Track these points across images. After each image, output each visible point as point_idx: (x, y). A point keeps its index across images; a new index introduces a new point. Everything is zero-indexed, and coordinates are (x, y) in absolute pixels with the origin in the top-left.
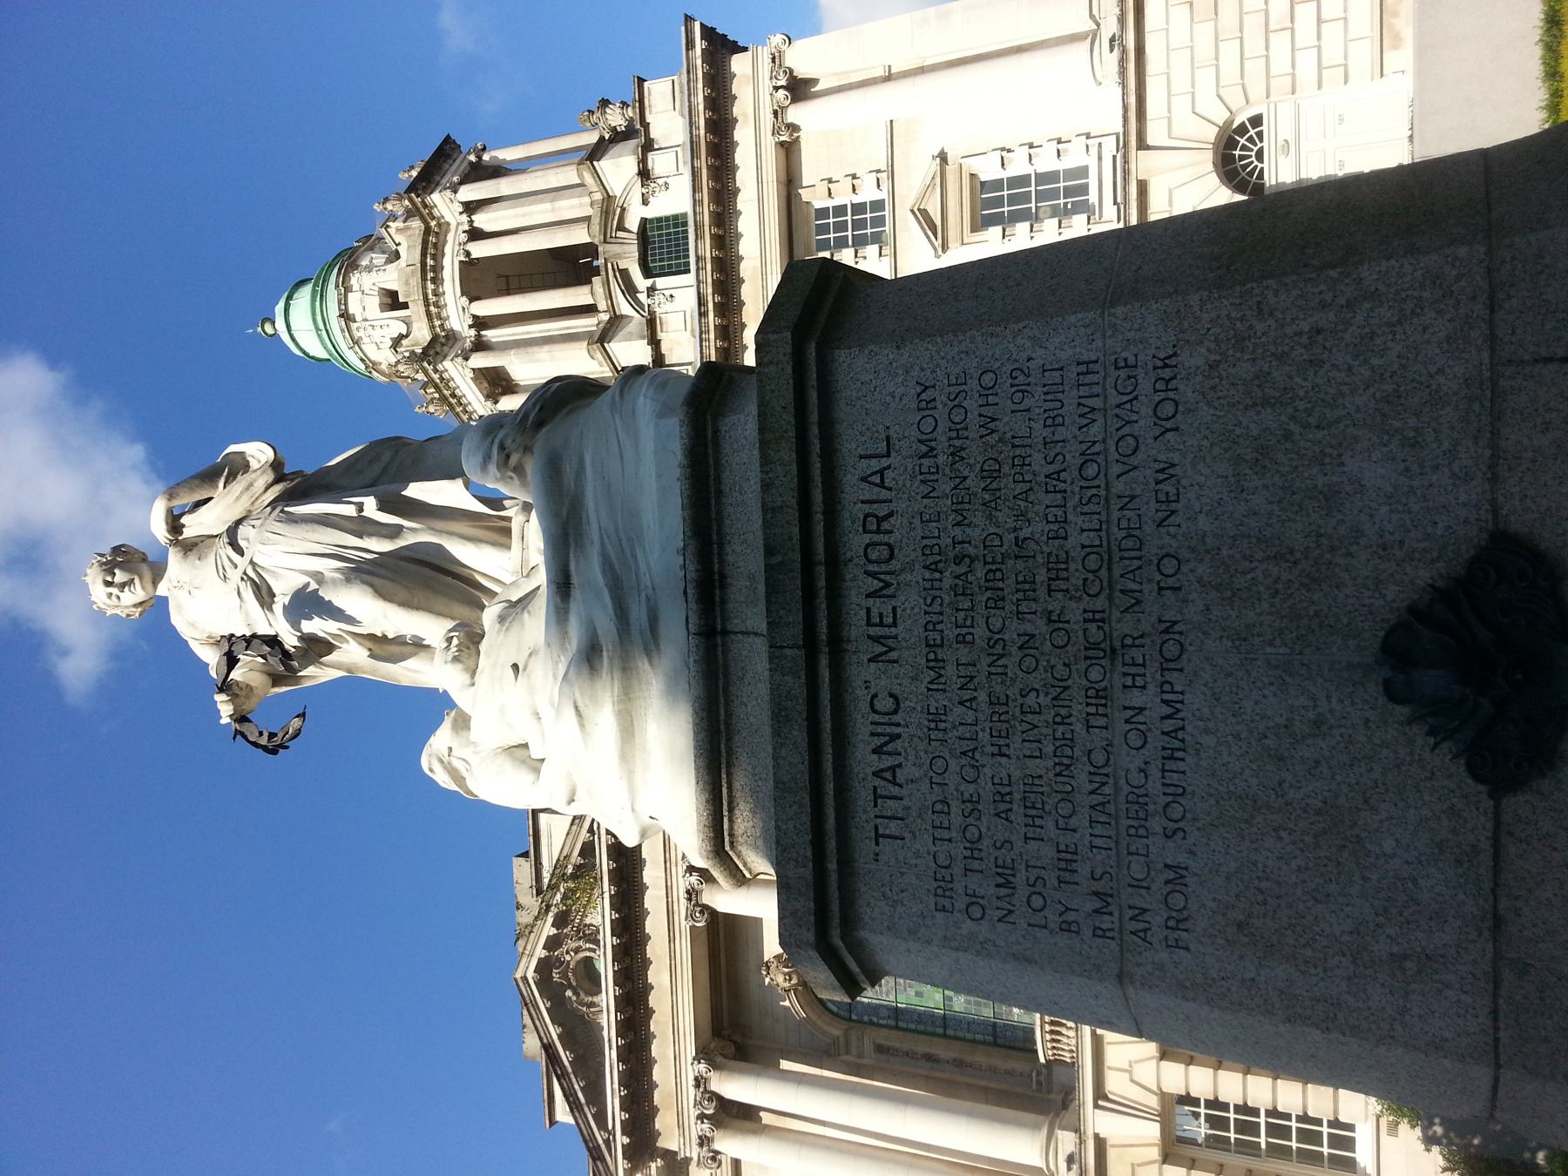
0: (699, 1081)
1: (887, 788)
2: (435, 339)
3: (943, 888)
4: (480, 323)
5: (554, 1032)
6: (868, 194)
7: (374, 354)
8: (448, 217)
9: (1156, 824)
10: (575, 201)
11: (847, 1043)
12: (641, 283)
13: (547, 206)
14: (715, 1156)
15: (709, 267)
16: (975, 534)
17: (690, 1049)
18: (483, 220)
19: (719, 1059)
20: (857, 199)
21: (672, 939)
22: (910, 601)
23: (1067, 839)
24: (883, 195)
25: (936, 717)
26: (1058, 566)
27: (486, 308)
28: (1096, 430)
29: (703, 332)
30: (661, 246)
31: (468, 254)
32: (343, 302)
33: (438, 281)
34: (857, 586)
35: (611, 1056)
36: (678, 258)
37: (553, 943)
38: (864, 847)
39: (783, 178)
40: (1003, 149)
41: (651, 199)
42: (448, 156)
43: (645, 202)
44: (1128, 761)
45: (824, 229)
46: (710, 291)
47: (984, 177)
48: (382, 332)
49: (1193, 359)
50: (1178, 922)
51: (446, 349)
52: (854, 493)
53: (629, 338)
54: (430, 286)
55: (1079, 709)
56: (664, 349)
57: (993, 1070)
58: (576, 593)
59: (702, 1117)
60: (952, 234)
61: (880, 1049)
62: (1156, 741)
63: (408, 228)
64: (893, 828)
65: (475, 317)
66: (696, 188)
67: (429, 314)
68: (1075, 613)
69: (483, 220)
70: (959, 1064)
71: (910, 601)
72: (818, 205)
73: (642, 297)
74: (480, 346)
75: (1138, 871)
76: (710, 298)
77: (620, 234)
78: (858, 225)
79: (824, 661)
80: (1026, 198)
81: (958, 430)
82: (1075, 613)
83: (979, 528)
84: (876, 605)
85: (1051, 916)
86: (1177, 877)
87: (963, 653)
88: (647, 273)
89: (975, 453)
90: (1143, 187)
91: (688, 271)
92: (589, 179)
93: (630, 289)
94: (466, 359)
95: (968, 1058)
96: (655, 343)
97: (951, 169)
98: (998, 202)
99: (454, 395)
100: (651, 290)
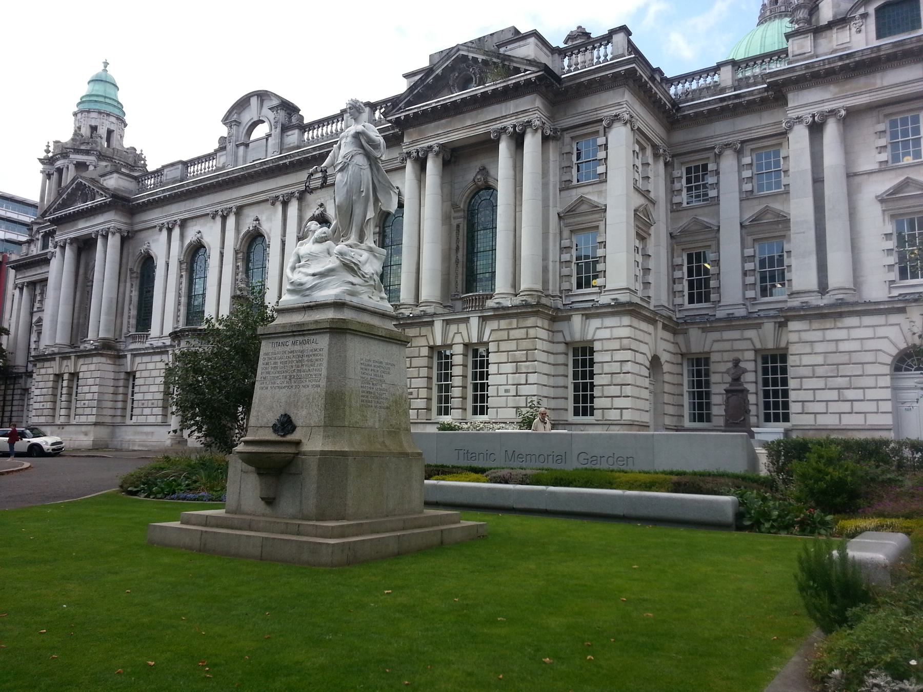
0: (430, 148)
5: (439, 71)
11: (458, 211)
14: (404, 160)
15: (873, 55)
17: (442, 141)
19: (441, 156)
21: (484, 123)
26: (300, 371)
34: (300, 339)
35: (432, 103)
37: (475, 60)
38: (271, 341)
45: (904, 122)
52: (312, 338)
56: (828, 33)
57: (457, 277)
59: (418, 152)
60: (891, 205)
61: (458, 226)
70: (457, 262)
73: (862, 11)
76: (852, 60)
83: (306, 359)
89: (314, 358)
90: (902, 310)
95: (460, 265)
96: (830, 26)
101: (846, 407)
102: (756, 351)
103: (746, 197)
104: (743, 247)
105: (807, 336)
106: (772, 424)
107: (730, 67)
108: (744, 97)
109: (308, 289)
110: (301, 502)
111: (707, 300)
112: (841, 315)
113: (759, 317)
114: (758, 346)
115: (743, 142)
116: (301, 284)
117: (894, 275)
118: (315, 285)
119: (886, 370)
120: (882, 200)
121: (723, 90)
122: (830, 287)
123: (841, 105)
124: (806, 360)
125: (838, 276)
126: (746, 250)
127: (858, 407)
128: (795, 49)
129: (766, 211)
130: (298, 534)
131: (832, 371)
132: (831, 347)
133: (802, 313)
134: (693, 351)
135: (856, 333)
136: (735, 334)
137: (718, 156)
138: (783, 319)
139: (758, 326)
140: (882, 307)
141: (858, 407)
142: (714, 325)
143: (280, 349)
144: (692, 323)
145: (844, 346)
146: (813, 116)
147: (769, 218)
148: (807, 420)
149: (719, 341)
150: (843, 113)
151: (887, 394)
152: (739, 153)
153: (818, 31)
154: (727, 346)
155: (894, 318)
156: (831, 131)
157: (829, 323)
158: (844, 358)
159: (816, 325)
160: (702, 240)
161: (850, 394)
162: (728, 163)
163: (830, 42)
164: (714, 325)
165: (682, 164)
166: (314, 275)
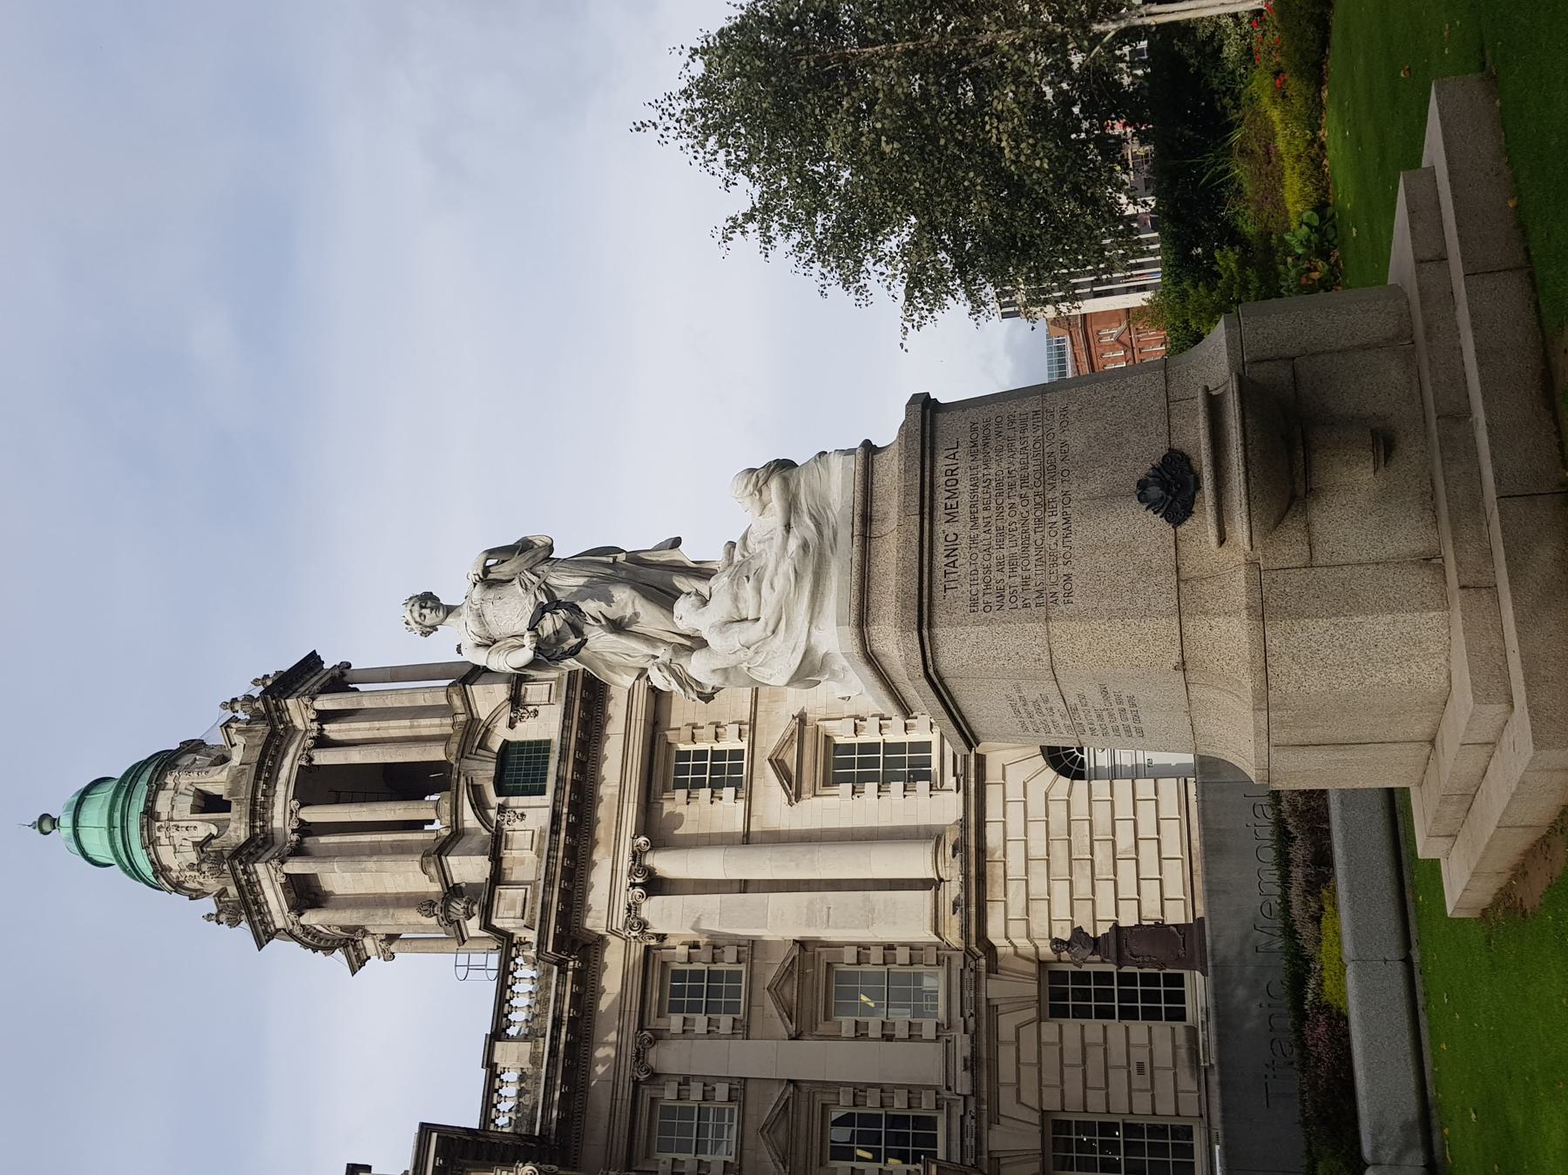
1: (949, 570)
2: (252, 839)
3: (974, 602)
4: (305, 829)
6: (729, 743)
7: (167, 856)
8: (298, 723)
9: (1060, 561)
10: (437, 721)
12: (494, 800)
13: (407, 723)
15: (568, 788)
16: (992, 471)
18: (333, 730)
20: (717, 747)
22: (965, 498)
23: (1026, 574)
24: (744, 745)
25: (973, 540)
26: (1024, 480)
27: (313, 815)
28: (1039, 433)
29: (553, 848)
30: (520, 769)
31: (311, 759)
32: (151, 800)
33: (271, 782)
36: (534, 781)
39: (651, 720)
40: (856, 717)
41: (518, 724)
42: (311, 669)
43: (512, 725)
44: (1049, 541)
45: (685, 770)
46: (565, 810)
47: (839, 740)
48: (185, 834)
49: (1073, 408)
50: (1069, 594)
51: (261, 851)
53: (469, 853)
54: (262, 786)
55: (1032, 525)
58: (794, 530)
60: (806, 785)
62: (1061, 532)
63: (250, 731)
64: (953, 584)
65: (301, 822)
66: (567, 715)
67: (253, 815)
68: (1031, 494)
69: (333, 730)
71: (965, 498)
72: (682, 747)
73: (492, 813)
74: (299, 851)
75: (1053, 579)
77: (480, 752)
78: (714, 769)
79: (926, 522)
80: (875, 763)
81: (986, 438)
82: (1031, 494)
84: (949, 502)
85: (1020, 604)
86: (1068, 577)
87: (986, 514)
88: (499, 794)
89: (993, 443)
91: (542, 792)
92: (457, 702)
93: (480, 805)
94: (283, 862)
97: (809, 728)
98: (850, 763)
99: (256, 902)
100: (502, 809)
101: (1148, 850)
102: (1040, 1020)
103: (743, 1029)
104: (838, 1038)
105: (1016, 910)
106: (1188, 1006)
107: (498, 1044)
108: (562, 1012)
109: (820, 533)
110: (1365, 348)
111: (931, 1122)
112: (981, 850)
113: (976, 1014)
114: (1032, 1013)
115: (641, 1028)
116: (805, 546)
117: (923, 786)
118: (812, 516)
119: (1080, 785)
120: (796, 796)
121: (535, 1059)
122: (931, 875)
123: (628, 839)
124: (1061, 910)
125: (916, 862)
126: (844, 1034)
127: (1147, 830)
128: (512, 914)
129: (775, 989)
130: (1442, 259)
131: (1082, 868)
132: (1038, 869)
133: (973, 909)
134: (1038, 1145)
135: (1015, 828)
136: (1006, 1058)
137: (654, 1076)
138: (981, 953)
139: (993, 1009)
140: (972, 786)
141: (1147, 830)
142: (985, 1096)
143: (963, 566)
144: (978, 1139)
145: (1038, 849)
146: (633, 885)
147: (791, 992)
148: (1175, 884)
149: (1018, 1091)
150: (642, 840)
151: (1123, 786)
152: (658, 1036)
153: (497, 877)
154: (1029, 1075)
155: (993, 773)
156: (666, 864)
157: (994, 871)
158: (1060, 850)
159: (994, 891)
160: (810, 1116)
161: (1125, 840)
162: (670, 1058)
163: (522, 862)
164: (985, 1096)
165: (648, 1156)
166: (788, 527)
